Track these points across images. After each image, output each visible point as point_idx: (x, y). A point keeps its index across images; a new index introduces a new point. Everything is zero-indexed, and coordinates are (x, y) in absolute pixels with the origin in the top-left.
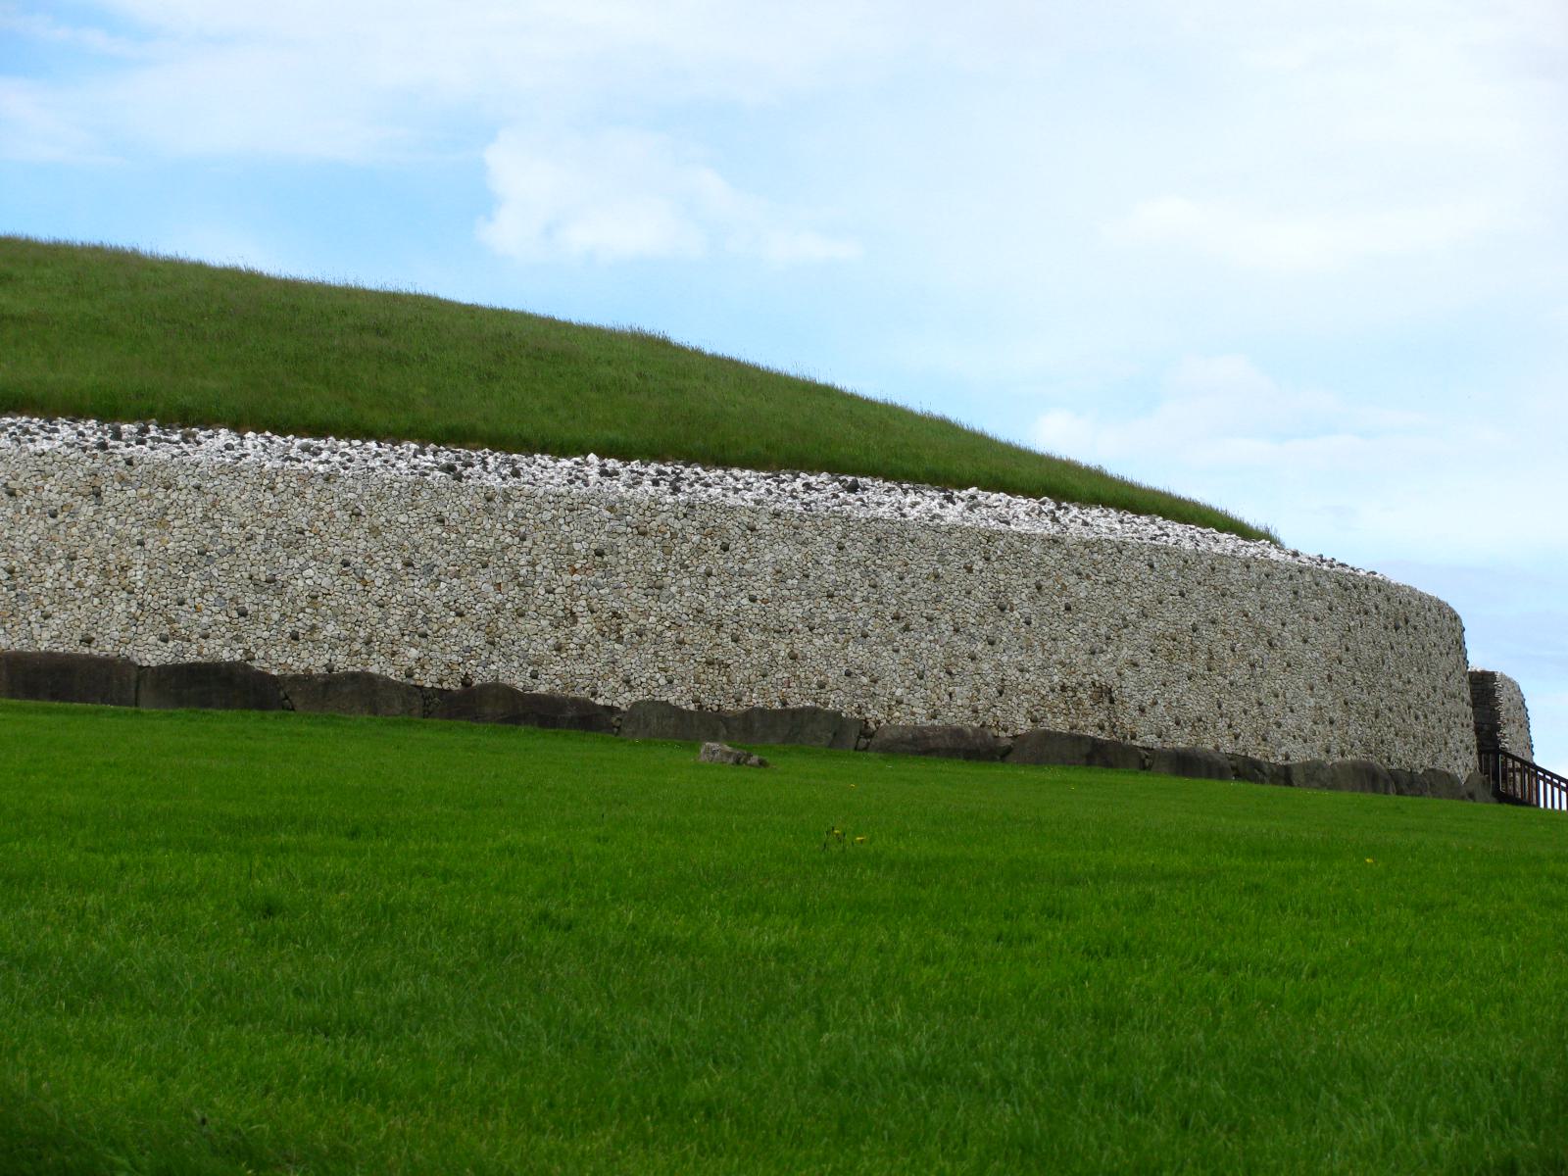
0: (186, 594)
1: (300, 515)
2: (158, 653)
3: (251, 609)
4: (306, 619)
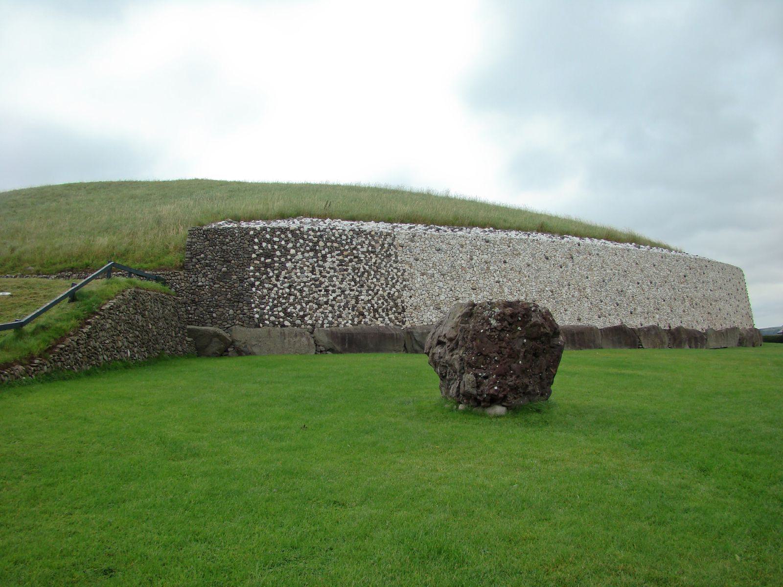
0: (602, 298)
1: (625, 265)
2: (599, 323)
3: (619, 302)
4: (633, 305)
